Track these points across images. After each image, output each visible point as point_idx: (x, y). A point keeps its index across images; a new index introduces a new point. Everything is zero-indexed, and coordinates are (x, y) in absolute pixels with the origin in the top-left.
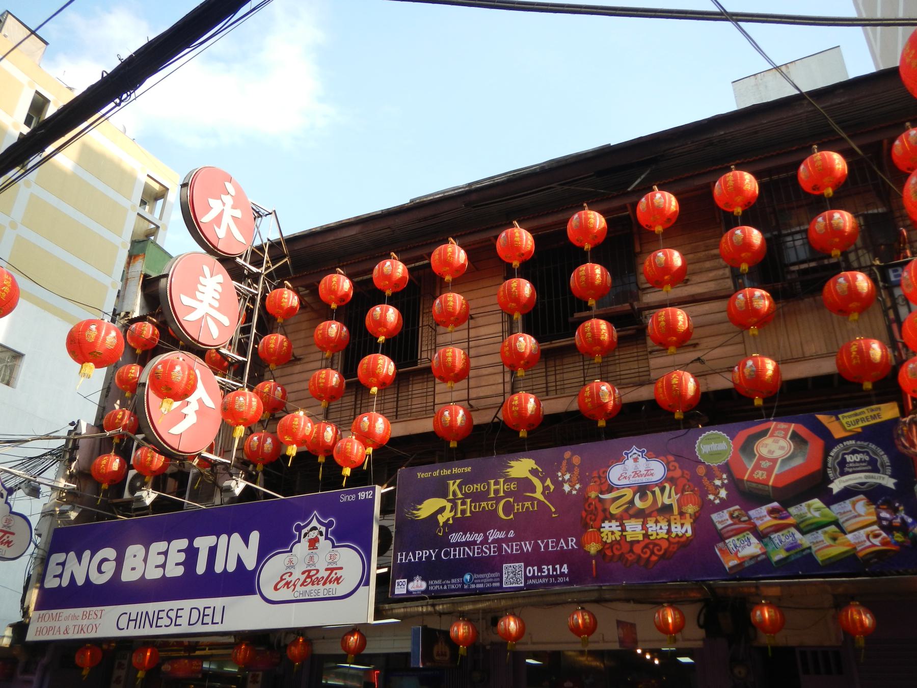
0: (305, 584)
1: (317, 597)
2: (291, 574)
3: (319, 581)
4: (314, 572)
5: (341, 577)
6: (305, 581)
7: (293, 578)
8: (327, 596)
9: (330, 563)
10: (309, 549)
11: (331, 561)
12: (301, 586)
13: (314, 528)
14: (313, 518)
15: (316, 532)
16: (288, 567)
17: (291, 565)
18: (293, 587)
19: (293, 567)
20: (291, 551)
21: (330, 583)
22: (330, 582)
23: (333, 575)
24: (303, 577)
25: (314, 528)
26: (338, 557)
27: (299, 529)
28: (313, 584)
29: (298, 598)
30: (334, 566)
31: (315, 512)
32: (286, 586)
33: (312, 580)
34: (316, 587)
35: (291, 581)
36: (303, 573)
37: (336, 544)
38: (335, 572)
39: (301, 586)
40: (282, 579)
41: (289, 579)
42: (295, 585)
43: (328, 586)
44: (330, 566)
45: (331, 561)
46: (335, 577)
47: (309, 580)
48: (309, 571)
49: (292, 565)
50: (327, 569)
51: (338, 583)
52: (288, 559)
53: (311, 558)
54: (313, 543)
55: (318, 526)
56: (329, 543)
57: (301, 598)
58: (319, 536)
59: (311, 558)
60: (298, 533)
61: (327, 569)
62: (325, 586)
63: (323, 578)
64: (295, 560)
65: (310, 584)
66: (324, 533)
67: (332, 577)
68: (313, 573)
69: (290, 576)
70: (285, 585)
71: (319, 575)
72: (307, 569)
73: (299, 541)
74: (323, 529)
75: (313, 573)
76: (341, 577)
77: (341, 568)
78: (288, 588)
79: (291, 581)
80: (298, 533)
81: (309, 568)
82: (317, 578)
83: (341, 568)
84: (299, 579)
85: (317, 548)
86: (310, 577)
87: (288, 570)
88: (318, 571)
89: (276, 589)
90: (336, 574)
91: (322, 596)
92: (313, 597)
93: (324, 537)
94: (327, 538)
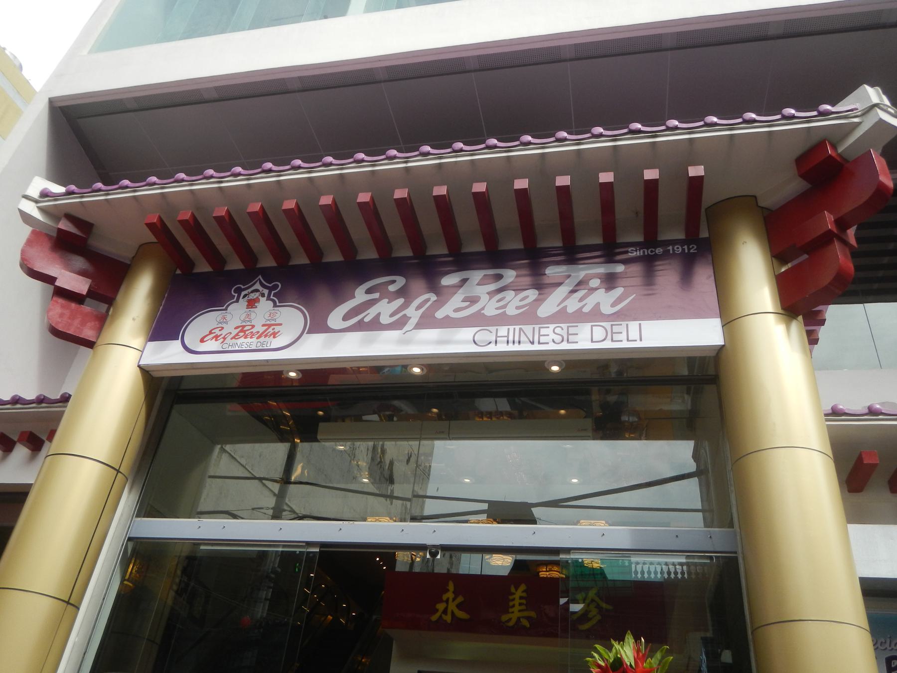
0: (237, 337)
1: (248, 348)
2: (223, 328)
4: (251, 327)
5: (279, 331)
6: (237, 335)
7: (224, 332)
8: (261, 348)
9: (269, 320)
10: (247, 308)
11: (270, 318)
12: (232, 339)
13: (257, 291)
14: (257, 281)
15: (257, 294)
16: (221, 323)
18: (222, 340)
19: (226, 323)
20: (226, 309)
22: (266, 336)
23: (270, 330)
24: (235, 332)
25: (257, 291)
26: (278, 315)
27: (238, 291)
28: (246, 338)
29: (227, 349)
30: (273, 322)
31: (260, 277)
32: (214, 339)
34: (249, 340)
35: (222, 334)
36: (236, 328)
37: (278, 304)
38: (272, 327)
39: (232, 339)
40: (211, 333)
41: (219, 333)
42: (224, 338)
43: (262, 339)
44: (268, 322)
45: (270, 318)
47: (241, 334)
48: (244, 326)
49: (224, 320)
50: (264, 325)
51: (274, 337)
52: (221, 316)
53: (248, 315)
55: (261, 288)
56: (271, 303)
57: (230, 349)
58: (260, 297)
59: (248, 315)
60: (236, 295)
61: (264, 325)
62: (259, 340)
63: (258, 332)
64: (228, 317)
65: (242, 339)
66: (266, 295)
67: (269, 332)
69: (220, 330)
70: (213, 338)
71: (254, 330)
72: (242, 325)
73: (237, 301)
74: (266, 292)
76: (279, 331)
77: (280, 324)
78: (216, 340)
79: (222, 334)
80: (236, 295)
81: (244, 324)
83: (280, 324)
84: (231, 333)
85: (256, 307)
87: (220, 325)
88: (253, 326)
90: (273, 329)
91: (254, 347)
92: (244, 349)
93: (265, 298)
94: (269, 299)
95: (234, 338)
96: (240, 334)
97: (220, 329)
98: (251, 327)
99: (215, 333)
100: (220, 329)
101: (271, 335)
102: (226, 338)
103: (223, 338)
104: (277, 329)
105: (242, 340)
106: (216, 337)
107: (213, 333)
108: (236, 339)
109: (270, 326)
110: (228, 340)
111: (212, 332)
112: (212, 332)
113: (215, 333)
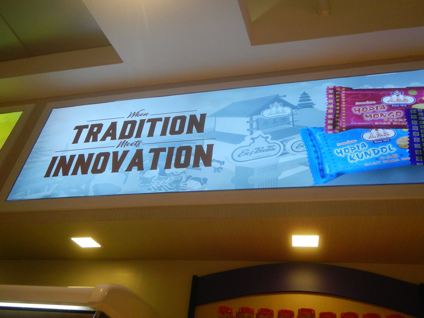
3: (264, 151)
4: (262, 148)
6: (257, 151)
7: (250, 151)
12: (254, 153)
18: (250, 154)
21: (269, 151)
22: (270, 150)
23: (271, 148)
28: (261, 152)
33: (260, 151)
35: (248, 153)
36: (255, 149)
38: (272, 147)
39: (254, 153)
41: (247, 152)
42: (251, 154)
46: (272, 148)
47: (259, 151)
50: (268, 147)
61: (268, 147)
63: (266, 149)
68: (260, 149)
75: (260, 149)
78: (247, 155)
82: (263, 150)
84: (253, 151)
91: (265, 156)
96: (258, 151)
97: (247, 150)
98: (262, 148)
99: (245, 152)
100: (247, 150)
101: (272, 150)
102: (252, 153)
103: (250, 154)
107: (244, 152)
108: (257, 153)
111: (244, 152)
112: (244, 152)
113: (245, 152)
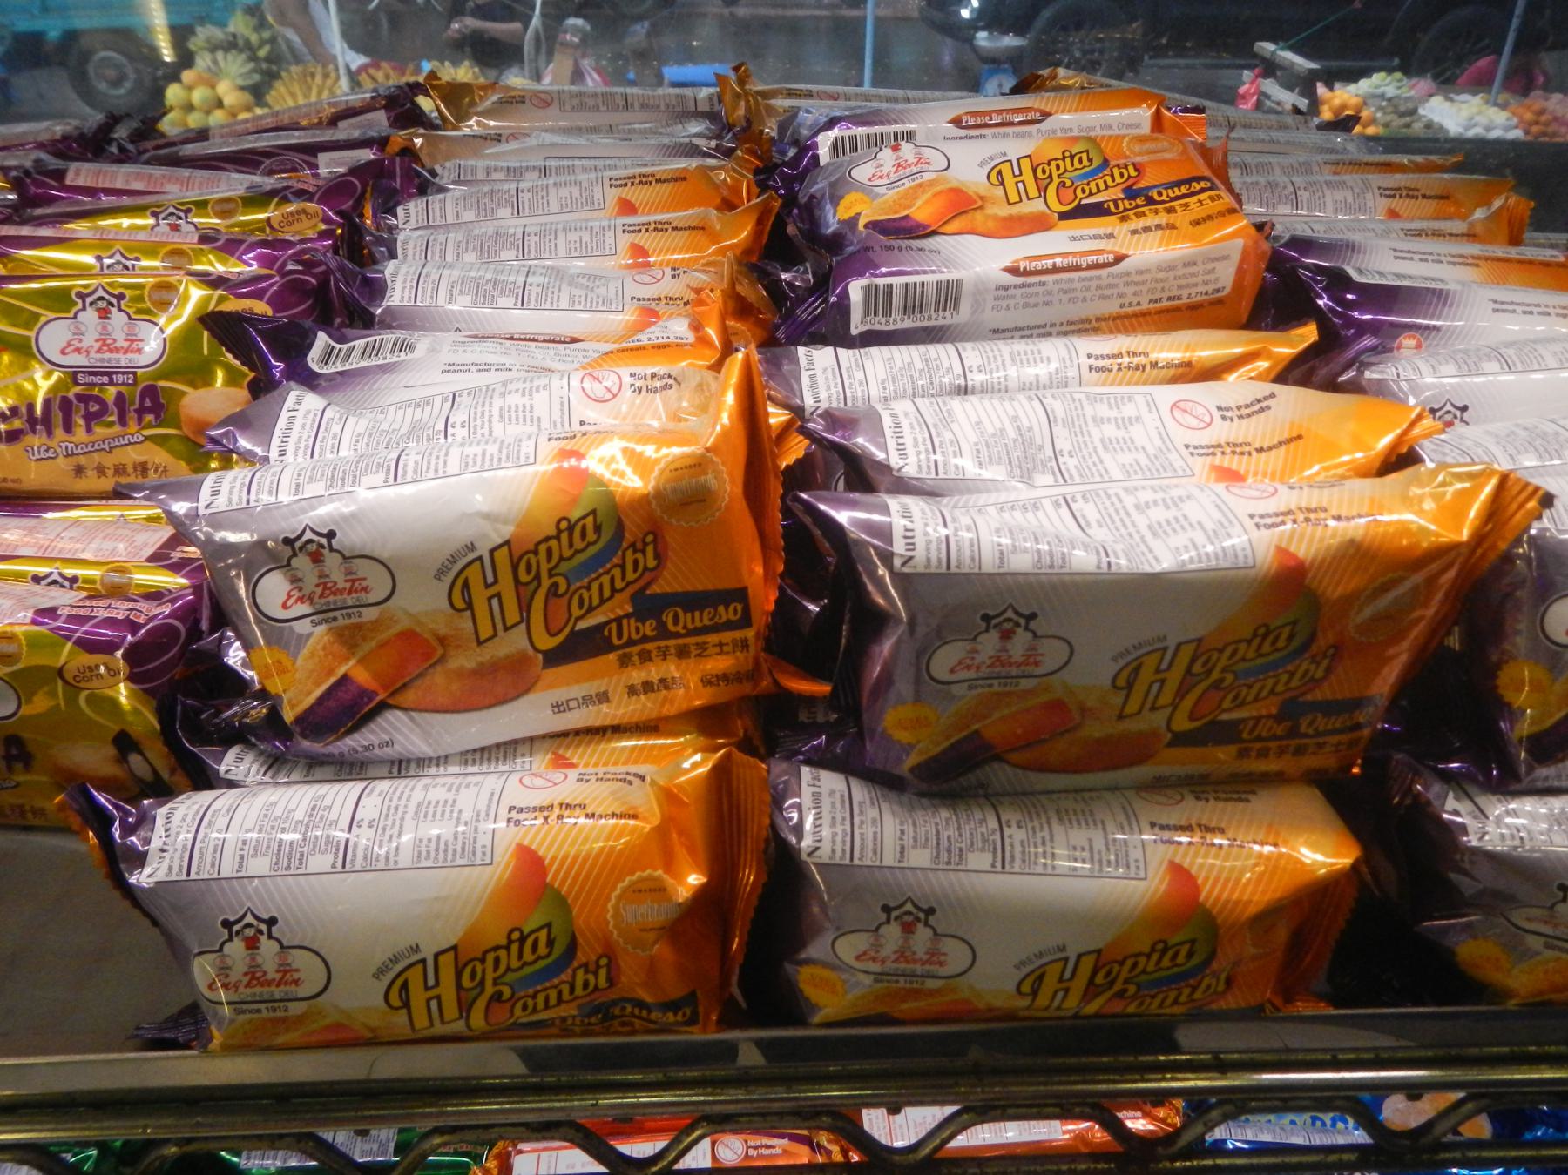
7: (84, 345)
17: (79, 335)
20: (75, 317)
24: (97, 345)
28: (111, 351)
34: (114, 356)
40: (69, 345)
42: (88, 352)
43: (130, 356)
53: (104, 328)
54: (104, 314)
59: (104, 328)
73: (84, 308)
74: (114, 301)
86: (105, 344)
89: (63, 352)
94: (120, 309)
95: (98, 351)
104: (140, 344)
105: (107, 356)
106: (78, 350)
109: (132, 341)
110: (93, 354)
